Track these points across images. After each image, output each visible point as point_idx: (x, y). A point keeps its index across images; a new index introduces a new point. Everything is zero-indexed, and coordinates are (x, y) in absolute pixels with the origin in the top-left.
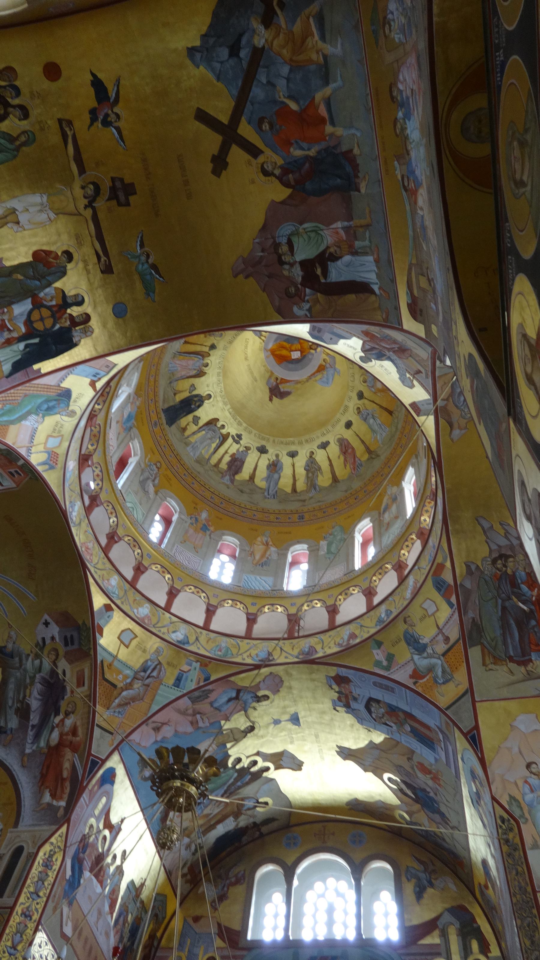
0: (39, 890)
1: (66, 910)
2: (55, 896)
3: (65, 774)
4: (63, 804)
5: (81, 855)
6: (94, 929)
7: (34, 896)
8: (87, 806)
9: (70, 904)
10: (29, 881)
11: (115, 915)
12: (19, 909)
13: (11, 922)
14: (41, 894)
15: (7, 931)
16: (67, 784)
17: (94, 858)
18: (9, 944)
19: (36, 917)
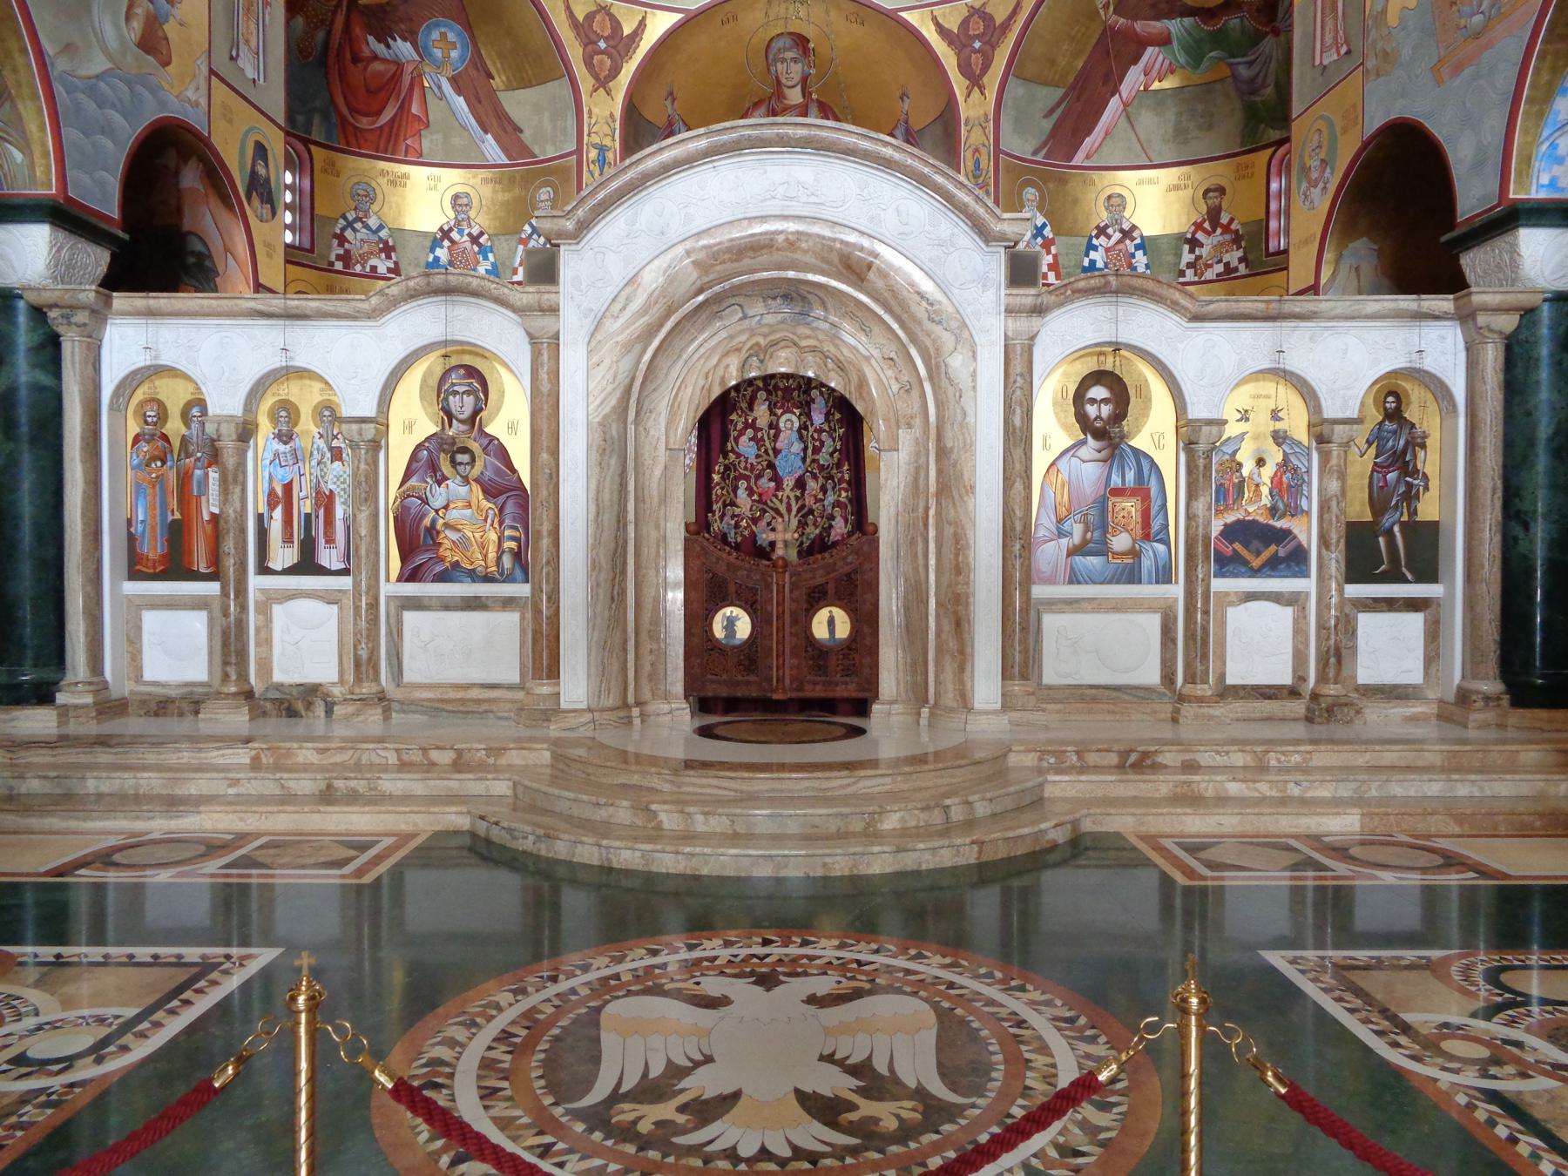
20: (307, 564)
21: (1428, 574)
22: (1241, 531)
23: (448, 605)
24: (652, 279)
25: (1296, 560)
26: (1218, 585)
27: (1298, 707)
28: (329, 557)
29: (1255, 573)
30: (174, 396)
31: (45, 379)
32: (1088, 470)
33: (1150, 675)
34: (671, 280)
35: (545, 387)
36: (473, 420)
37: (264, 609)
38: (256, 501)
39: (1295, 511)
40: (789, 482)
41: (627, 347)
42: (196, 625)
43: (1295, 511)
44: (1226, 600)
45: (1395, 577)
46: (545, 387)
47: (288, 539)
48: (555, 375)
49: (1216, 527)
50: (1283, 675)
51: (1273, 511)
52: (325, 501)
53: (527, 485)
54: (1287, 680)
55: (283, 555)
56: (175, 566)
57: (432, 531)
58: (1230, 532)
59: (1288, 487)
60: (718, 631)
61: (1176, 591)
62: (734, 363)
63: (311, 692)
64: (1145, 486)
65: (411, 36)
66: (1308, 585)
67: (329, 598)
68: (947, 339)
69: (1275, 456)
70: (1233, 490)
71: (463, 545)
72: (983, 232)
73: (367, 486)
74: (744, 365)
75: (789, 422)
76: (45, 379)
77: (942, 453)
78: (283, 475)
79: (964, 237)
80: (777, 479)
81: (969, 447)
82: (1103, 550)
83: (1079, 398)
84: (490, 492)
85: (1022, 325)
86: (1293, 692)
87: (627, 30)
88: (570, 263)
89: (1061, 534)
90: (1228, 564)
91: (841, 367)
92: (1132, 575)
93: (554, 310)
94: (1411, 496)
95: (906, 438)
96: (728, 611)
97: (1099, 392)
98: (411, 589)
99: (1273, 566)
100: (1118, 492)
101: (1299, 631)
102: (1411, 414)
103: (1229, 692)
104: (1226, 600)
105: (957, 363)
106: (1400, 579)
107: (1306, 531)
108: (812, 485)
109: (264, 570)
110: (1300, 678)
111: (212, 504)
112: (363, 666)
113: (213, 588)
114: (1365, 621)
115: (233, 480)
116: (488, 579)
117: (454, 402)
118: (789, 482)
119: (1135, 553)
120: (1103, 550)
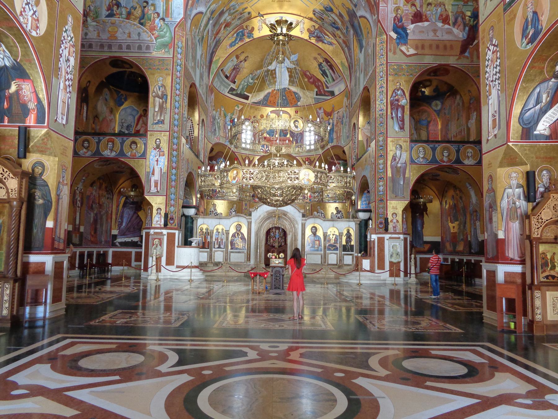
0: (382, 53)
1: (403, 48)
2: (390, 49)
3: (373, 3)
4: (376, 16)
5: (400, 24)
6: (436, 38)
7: (382, 57)
8: (387, 7)
9: (405, 44)
10: (377, 54)
11: (451, 22)
12: (378, 65)
13: (377, 71)
14: (383, 54)
15: (377, 74)
16: (375, 6)
17: (411, 18)
18: (379, 77)
19: (385, 62)
20: (219, 247)
21: (352, 251)
22: (330, 245)
23: (236, 252)
24: (262, 216)
25: (336, 249)
26: (327, 252)
27: (337, 267)
28: (222, 246)
29: (332, 250)
30: (204, 227)
31: (192, 225)
32: (312, 238)
33: (320, 262)
34: (264, 216)
35: (249, 227)
36: (240, 230)
37: (214, 253)
38: (214, 240)
39: (337, 243)
40: (277, 238)
41: (259, 223)
42: (206, 254)
43: (337, 243)
44: (328, 254)
45: (348, 251)
46: (249, 227)
47: (217, 244)
48: (251, 226)
49: (327, 245)
50: (336, 263)
51: (334, 243)
52: (222, 240)
53: (246, 238)
54: (336, 263)
55: (217, 246)
56: (203, 247)
57: (234, 243)
58: (329, 245)
59: (336, 240)
60: (268, 256)
61: (323, 252)
62: (271, 225)
63: (219, 263)
64: (319, 240)
65: (216, 160)
66: (338, 252)
67: (223, 251)
68: (295, 223)
69: (334, 236)
70: (329, 240)
71: (238, 245)
72: (300, 212)
73: (227, 238)
74: (272, 225)
75: (277, 231)
76: (192, 225)
77: (295, 236)
78: (217, 237)
79: (297, 212)
80: (276, 238)
81: (297, 235)
82: (314, 247)
83: (311, 229)
84: (241, 239)
85: (303, 222)
86: (336, 265)
87: (251, 159)
88: (253, 214)
89: (309, 245)
90: (329, 249)
91: (283, 226)
92: (317, 250)
93: (251, 219)
94: (350, 242)
95: (291, 234)
96: (270, 254)
97: (314, 229)
98: (232, 250)
99: (334, 250)
100: (316, 240)
101: (337, 257)
102: (350, 232)
103: (329, 265)
104: (328, 254)
105: (296, 226)
106: (349, 251)
107: (338, 246)
108: (280, 239)
109: (214, 248)
110: (337, 263)
111: (209, 240)
112: (226, 260)
113: (209, 250)
114: (345, 256)
115: (211, 237)
116: (241, 249)
117: (238, 228)
118: (277, 238)
119: (318, 248)
120: (314, 247)
